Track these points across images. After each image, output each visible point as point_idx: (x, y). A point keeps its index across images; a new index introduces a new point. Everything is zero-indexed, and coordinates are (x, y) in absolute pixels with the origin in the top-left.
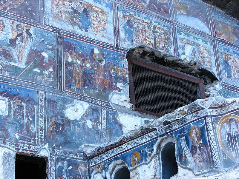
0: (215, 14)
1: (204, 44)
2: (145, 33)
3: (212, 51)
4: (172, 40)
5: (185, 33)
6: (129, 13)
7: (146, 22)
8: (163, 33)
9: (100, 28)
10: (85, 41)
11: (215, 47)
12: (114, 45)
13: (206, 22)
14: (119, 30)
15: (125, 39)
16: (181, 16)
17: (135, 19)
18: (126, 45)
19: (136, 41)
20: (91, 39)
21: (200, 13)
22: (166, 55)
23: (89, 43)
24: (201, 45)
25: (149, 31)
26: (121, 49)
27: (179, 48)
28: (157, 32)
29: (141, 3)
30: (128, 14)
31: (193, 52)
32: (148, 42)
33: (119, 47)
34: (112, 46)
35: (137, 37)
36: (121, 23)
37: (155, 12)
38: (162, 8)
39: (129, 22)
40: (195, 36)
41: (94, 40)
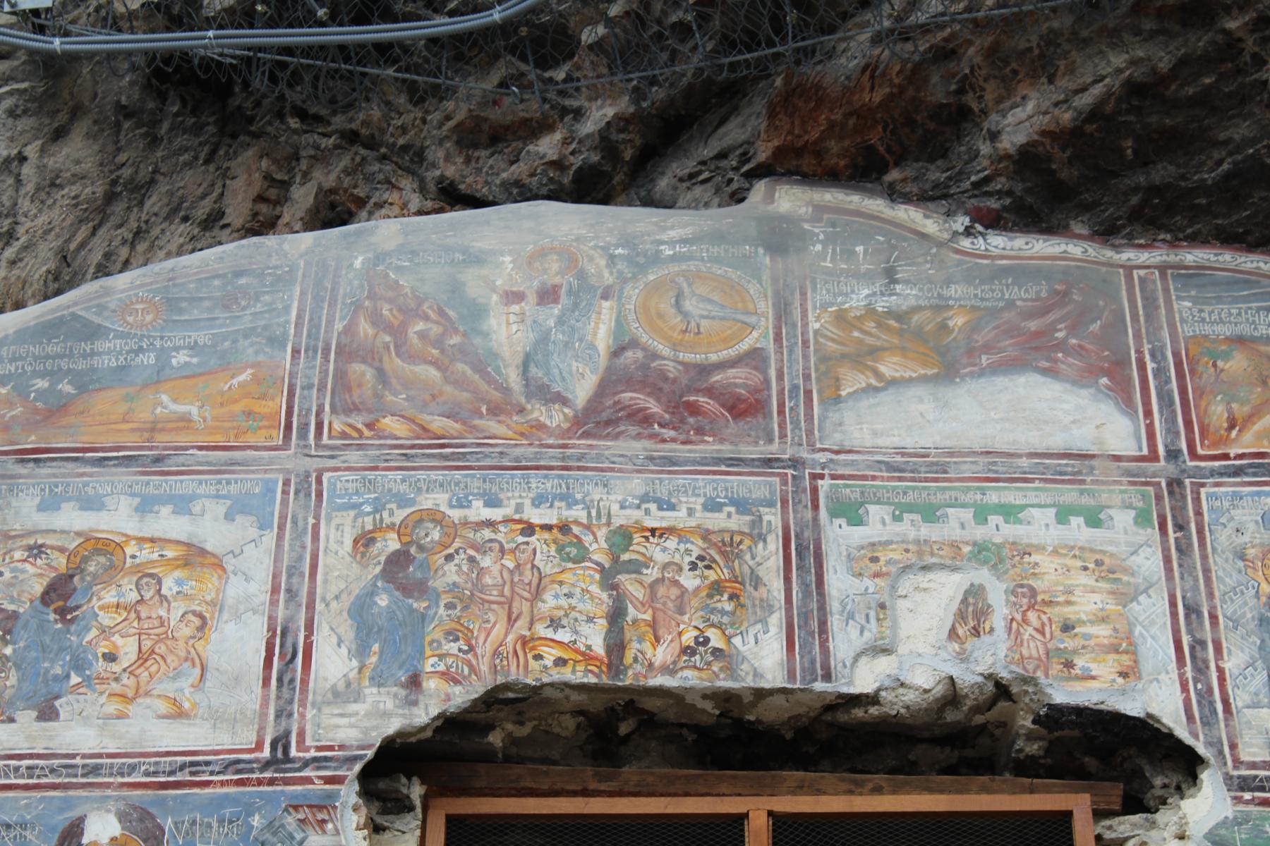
0: (1195, 301)
1: (1078, 530)
2: (537, 594)
3: (1149, 562)
4: (776, 586)
5: (898, 505)
6: (412, 502)
7: (547, 528)
8: (695, 554)
9: (154, 668)
10: (27, 787)
11: (1180, 527)
12: (259, 746)
13: (1104, 381)
14: (307, 637)
15: (348, 685)
16: (885, 397)
17: (451, 530)
18: (351, 726)
19: (446, 676)
20: (73, 756)
21: (1060, 335)
22: (726, 698)
23: (54, 787)
24: (1040, 548)
25: (563, 577)
26: (306, 764)
27: (835, 622)
28: (635, 568)
29: (522, 410)
30: (400, 515)
31: (961, 616)
32: (550, 654)
33: (293, 753)
34: (238, 762)
35: (453, 647)
36: (334, 589)
37: (638, 437)
38: (710, 392)
39: (398, 561)
40: (993, 498)
41: (100, 756)
